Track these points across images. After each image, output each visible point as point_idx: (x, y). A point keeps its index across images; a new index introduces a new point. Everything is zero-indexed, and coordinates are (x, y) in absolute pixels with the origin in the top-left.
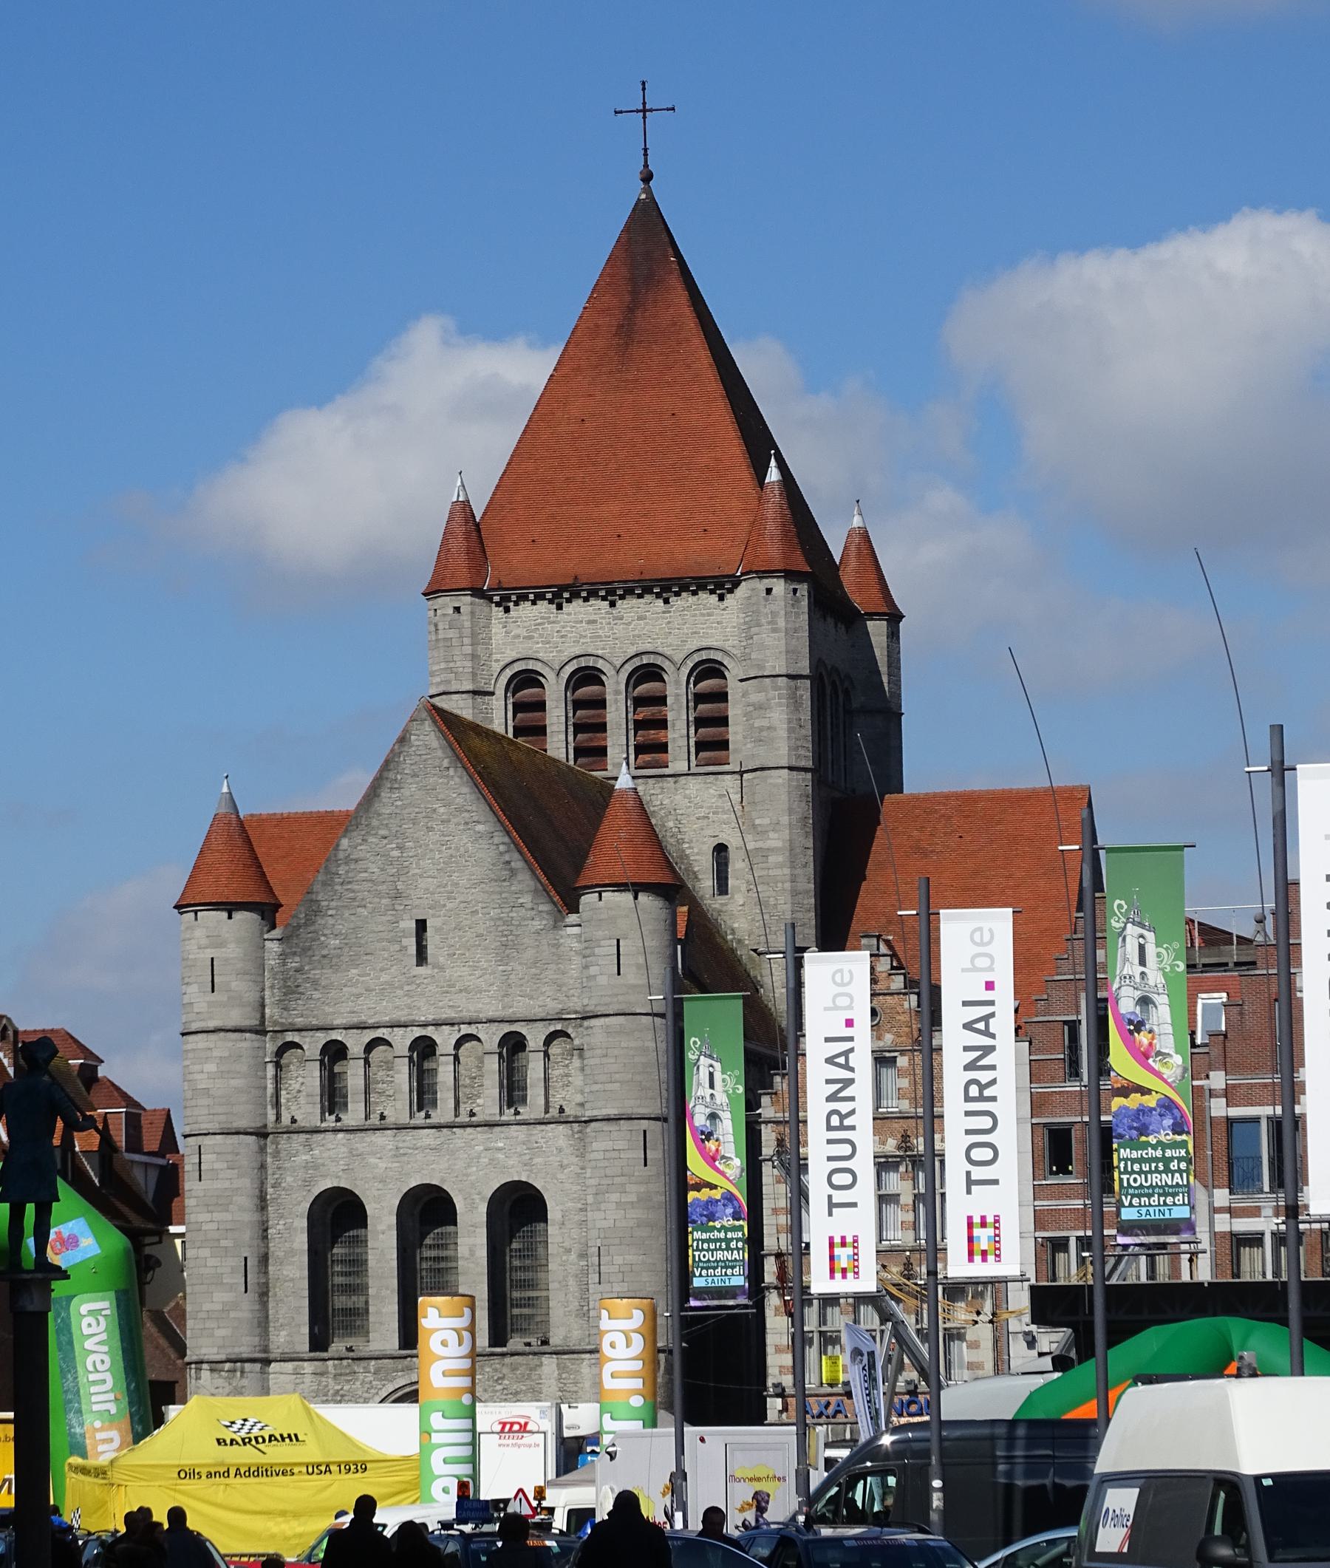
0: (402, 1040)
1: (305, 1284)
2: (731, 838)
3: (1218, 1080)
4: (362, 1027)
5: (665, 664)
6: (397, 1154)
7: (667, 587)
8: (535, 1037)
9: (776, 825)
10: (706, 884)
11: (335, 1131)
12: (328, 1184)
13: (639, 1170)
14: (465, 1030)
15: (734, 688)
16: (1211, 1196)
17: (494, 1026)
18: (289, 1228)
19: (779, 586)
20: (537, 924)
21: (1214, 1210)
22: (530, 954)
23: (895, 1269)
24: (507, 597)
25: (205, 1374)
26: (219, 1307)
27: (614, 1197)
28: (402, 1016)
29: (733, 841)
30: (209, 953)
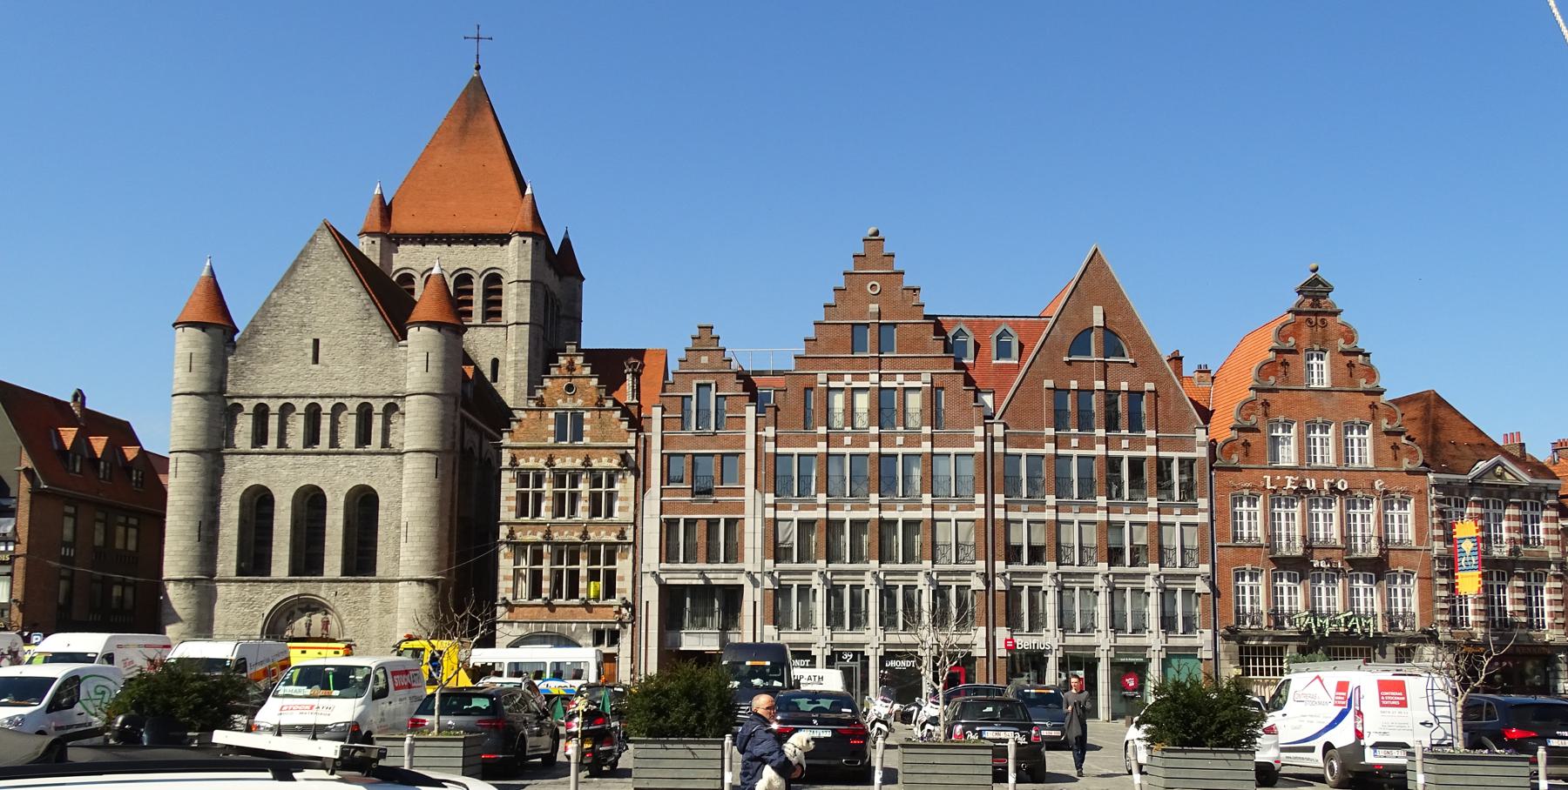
0: (301, 405)
1: (236, 538)
3: (770, 432)
6: (295, 467)
8: (378, 406)
15: (504, 286)
19: (529, 240)
20: (383, 344)
21: (765, 506)
28: (299, 391)
29: (500, 358)
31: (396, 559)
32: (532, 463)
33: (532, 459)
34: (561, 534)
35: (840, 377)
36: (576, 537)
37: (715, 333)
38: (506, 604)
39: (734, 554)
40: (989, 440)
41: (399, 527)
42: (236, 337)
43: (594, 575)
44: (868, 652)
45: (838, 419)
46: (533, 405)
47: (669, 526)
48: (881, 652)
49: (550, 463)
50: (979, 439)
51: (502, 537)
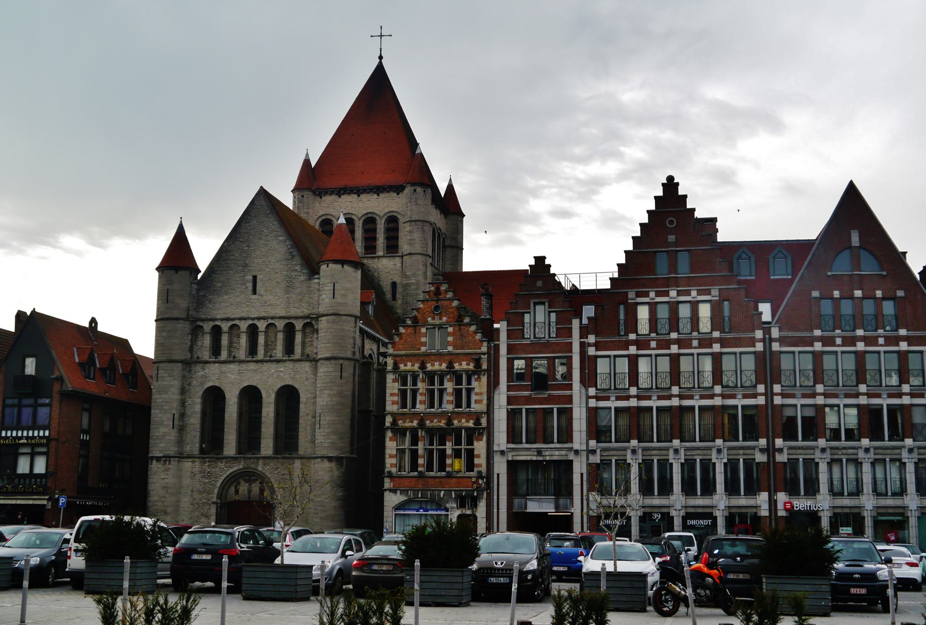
0: (244, 326)
1: (198, 426)
2: (397, 279)
3: (592, 339)
4: (228, 319)
5: (377, 218)
7: (378, 190)
8: (299, 325)
9: (414, 275)
10: (389, 296)
11: (215, 362)
12: (210, 384)
13: (338, 381)
14: (270, 321)
15: (401, 226)
16: (587, 390)
17: (282, 321)
18: (194, 403)
19: (419, 190)
20: (302, 278)
21: (589, 397)
22: (299, 290)
23: (443, 422)
24: (320, 193)
25: (154, 462)
26: (160, 434)
27: (327, 392)
28: (244, 315)
30: (167, 287)
31: (313, 441)
32: (409, 366)
33: (409, 364)
34: (432, 421)
35: (646, 295)
36: (443, 424)
37: (547, 262)
38: (390, 475)
39: (566, 435)
40: (768, 340)
41: (314, 417)
42: (199, 276)
43: (457, 454)
44: (673, 513)
45: (643, 327)
46: (409, 322)
47: (513, 416)
48: (682, 513)
49: (423, 366)
50: (760, 340)
51: (388, 424)
